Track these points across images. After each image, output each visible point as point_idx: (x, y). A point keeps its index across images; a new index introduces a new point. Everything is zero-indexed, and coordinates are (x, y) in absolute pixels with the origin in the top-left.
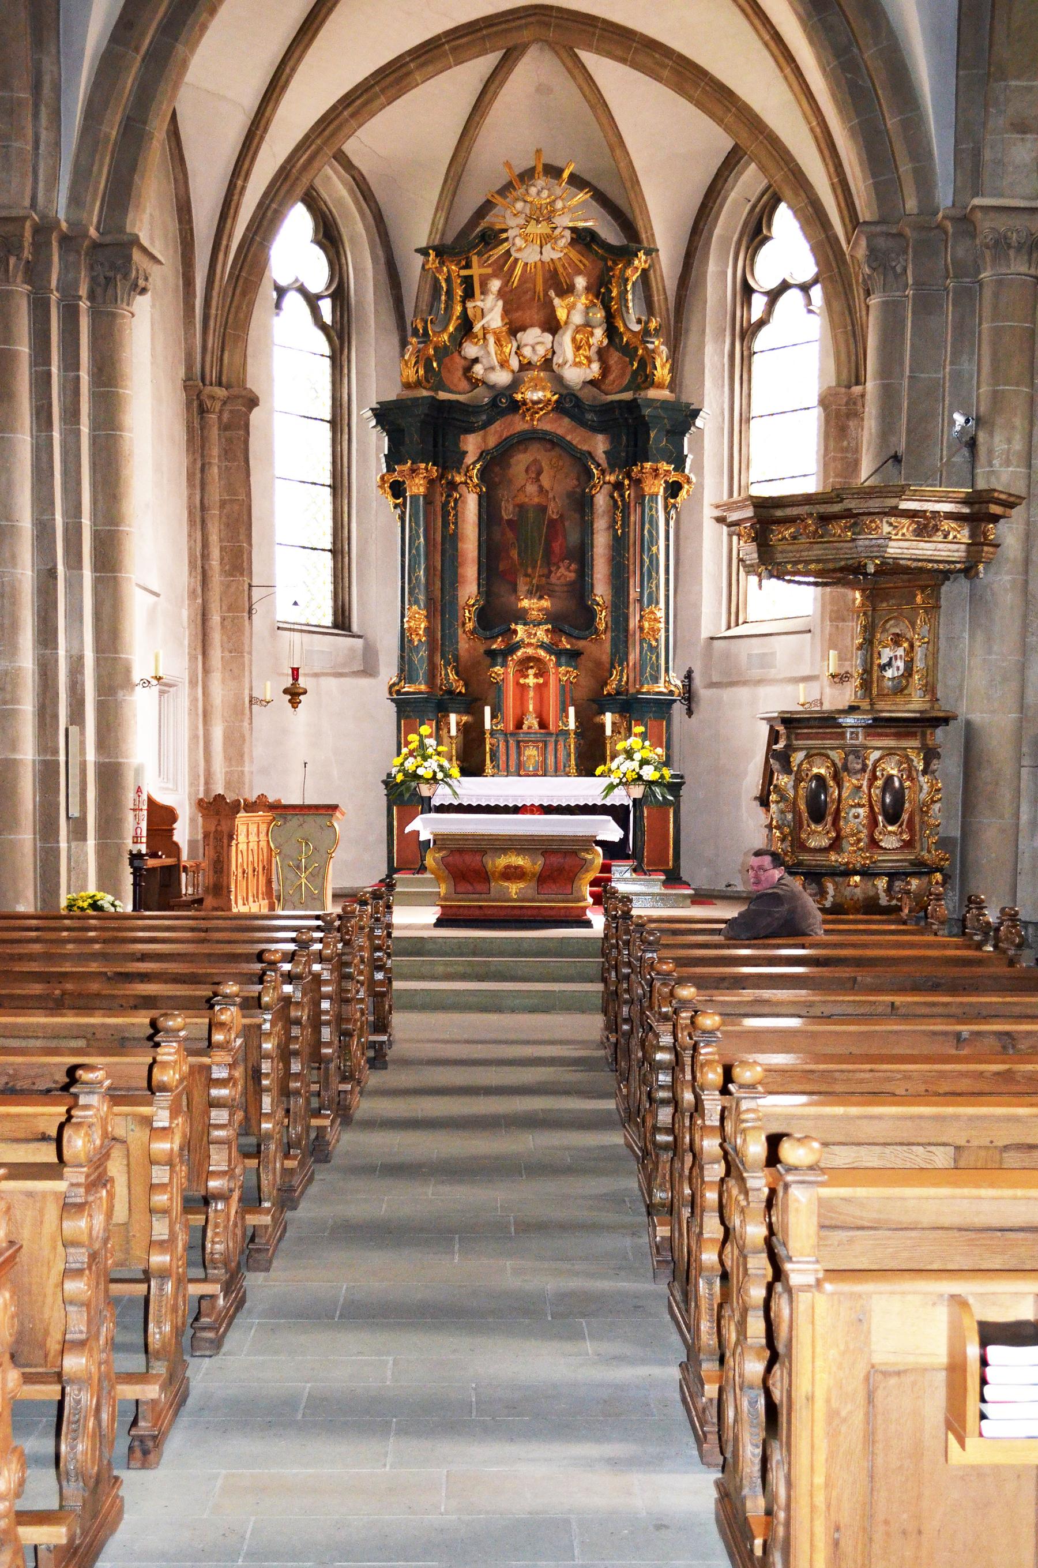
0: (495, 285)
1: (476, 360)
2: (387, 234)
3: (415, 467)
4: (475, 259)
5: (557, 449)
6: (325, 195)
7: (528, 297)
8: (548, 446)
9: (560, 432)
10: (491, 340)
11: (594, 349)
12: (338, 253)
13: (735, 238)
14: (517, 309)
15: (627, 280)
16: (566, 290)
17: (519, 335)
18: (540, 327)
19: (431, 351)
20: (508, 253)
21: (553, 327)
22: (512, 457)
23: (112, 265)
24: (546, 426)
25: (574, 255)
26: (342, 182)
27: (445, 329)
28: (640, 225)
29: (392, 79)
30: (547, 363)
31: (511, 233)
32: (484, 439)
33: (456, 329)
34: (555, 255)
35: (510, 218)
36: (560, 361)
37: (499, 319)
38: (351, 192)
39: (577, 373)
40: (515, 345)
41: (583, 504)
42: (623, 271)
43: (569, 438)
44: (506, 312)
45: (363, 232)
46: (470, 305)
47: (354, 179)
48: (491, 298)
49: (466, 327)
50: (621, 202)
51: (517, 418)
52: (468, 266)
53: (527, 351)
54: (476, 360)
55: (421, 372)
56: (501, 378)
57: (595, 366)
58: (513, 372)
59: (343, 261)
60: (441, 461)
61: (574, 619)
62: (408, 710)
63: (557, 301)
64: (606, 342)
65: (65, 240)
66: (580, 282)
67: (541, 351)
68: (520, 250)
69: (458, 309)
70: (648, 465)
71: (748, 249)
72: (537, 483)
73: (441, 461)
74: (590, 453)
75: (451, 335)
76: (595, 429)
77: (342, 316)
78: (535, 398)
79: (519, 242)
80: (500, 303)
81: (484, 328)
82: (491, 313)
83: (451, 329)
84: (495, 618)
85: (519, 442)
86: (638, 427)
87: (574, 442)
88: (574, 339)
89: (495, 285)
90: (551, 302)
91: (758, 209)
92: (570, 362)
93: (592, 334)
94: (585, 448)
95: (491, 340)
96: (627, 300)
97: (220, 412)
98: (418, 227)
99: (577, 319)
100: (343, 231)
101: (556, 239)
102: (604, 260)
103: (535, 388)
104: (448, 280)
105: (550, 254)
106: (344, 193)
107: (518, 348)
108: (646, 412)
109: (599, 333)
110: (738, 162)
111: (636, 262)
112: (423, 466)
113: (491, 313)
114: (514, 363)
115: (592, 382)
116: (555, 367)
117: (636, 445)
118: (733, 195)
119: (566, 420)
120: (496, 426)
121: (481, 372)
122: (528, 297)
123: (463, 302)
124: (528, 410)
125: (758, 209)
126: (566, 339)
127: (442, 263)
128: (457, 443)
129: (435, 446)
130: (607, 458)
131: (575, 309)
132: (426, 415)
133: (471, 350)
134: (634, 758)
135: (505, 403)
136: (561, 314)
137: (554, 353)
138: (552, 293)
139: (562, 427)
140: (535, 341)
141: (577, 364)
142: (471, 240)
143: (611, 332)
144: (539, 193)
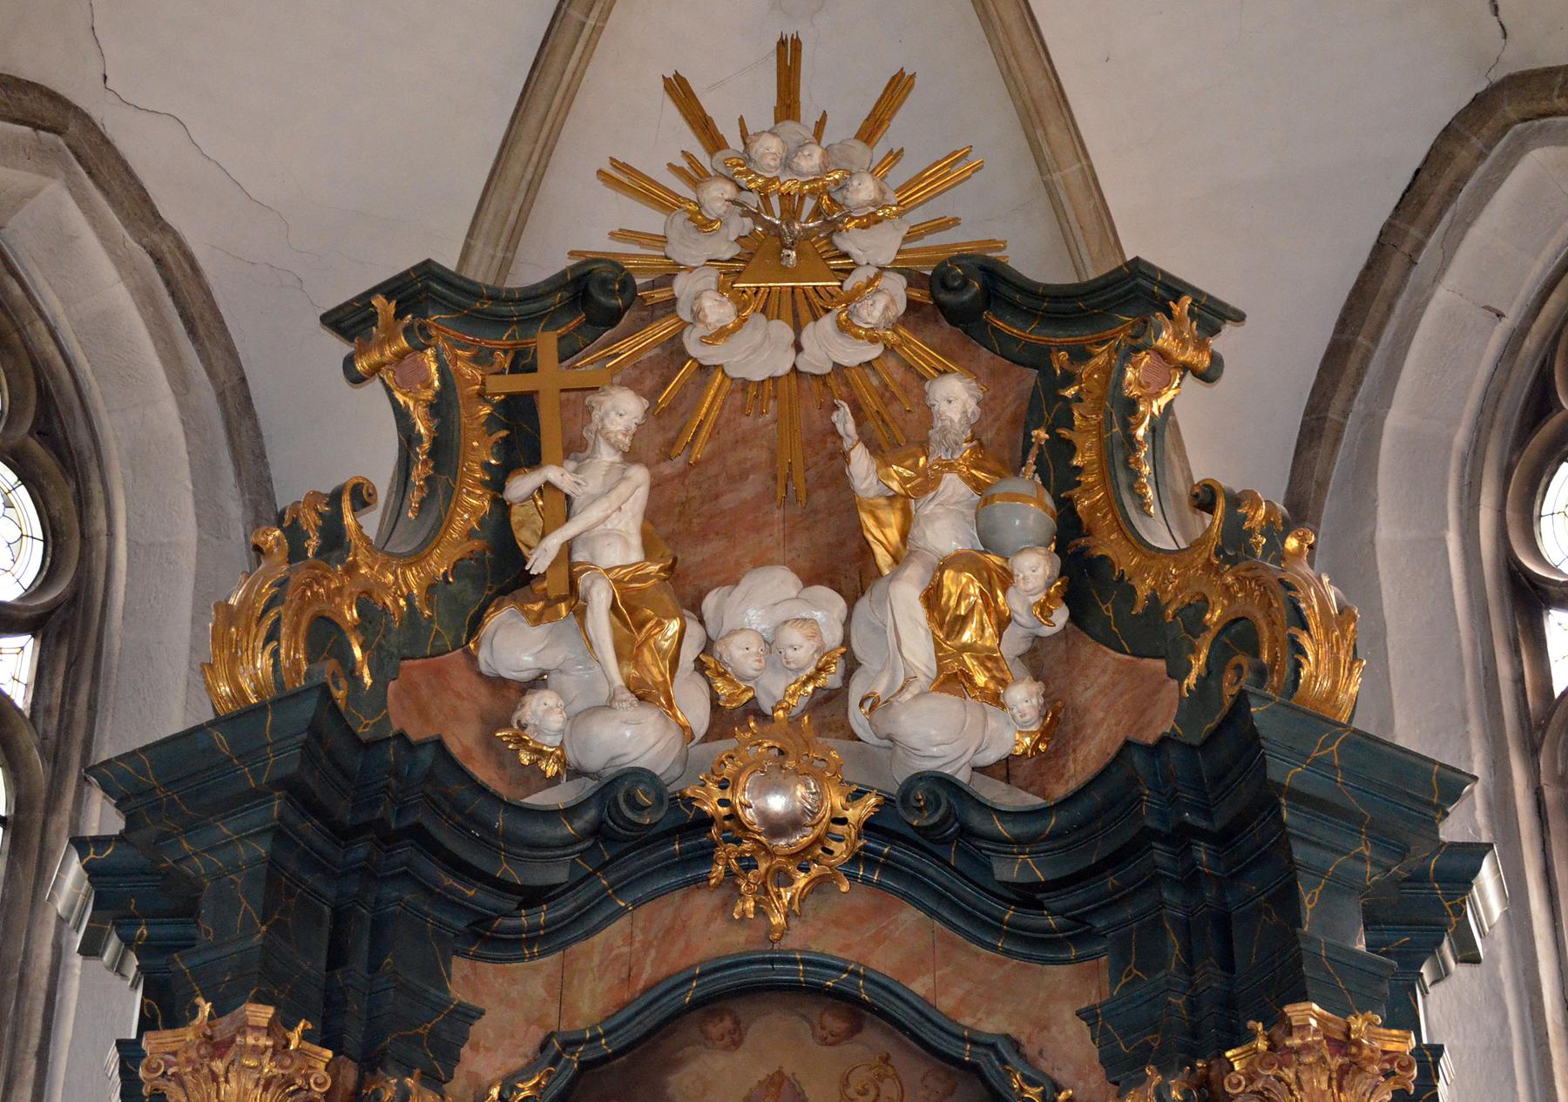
0: (622, 411)
1: (538, 682)
2: (261, 456)
3: (225, 1025)
4: (546, 343)
5: (874, 1039)
6: (51, 302)
7: (750, 489)
8: (837, 1025)
9: (883, 962)
10: (600, 597)
11: (1013, 644)
12: (82, 502)
13: (1461, 437)
14: (703, 536)
15: (1131, 405)
16: (899, 431)
17: (710, 603)
18: (797, 572)
19: (351, 614)
20: (674, 351)
21: (848, 570)
22: (675, 1064)
24: (829, 945)
25: (919, 349)
26: (119, 261)
27: (416, 557)
30: (828, 706)
31: (682, 286)
32: (560, 990)
33: (457, 568)
34: (854, 353)
36: (880, 689)
37: (636, 541)
38: (145, 298)
39: (946, 736)
40: (694, 632)
42: (1113, 378)
43: (919, 986)
44: (663, 524)
45: (178, 430)
46: (521, 486)
47: (159, 261)
48: (607, 456)
49: (501, 571)
51: (703, 902)
52: (523, 363)
53: (741, 654)
54: (538, 682)
55: (293, 652)
56: (635, 739)
57: (1024, 697)
58: (686, 731)
59: (101, 523)
60: (354, 1036)
63: (861, 465)
64: (1061, 616)
66: (955, 399)
67: (801, 650)
68: (723, 333)
69: (474, 503)
70: (1309, 1014)
71: (1506, 475)
73: (354, 1036)
74: (1015, 1045)
75: (431, 588)
76: (1039, 946)
77: (70, 691)
78: (777, 803)
79: (718, 311)
80: (639, 475)
81: (568, 548)
82: (603, 513)
83: (439, 564)
85: (709, 1004)
87: (946, 1003)
88: (932, 597)
89: (622, 411)
90: (846, 457)
91: (1530, 343)
92: (922, 682)
93: (1006, 579)
94: (991, 1025)
95: (600, 597)
96: (1135, 475)
99: (945, 529)
100: (110, 427)
101: (852, 298)
102: (1038, 359)
103: (775, 775)
104: (442, 408)
105: (826, 346)
106: (118, 295)
107: (708, 646)
108: (1285, 772)
109: (1035, 570)
110: (1454, 191)
111: (1165, 339)
112: (262, 1014)
113: (603, 513)
114: (695, 709)
115: (1005, 769)
116: (858, 718)
117: (1228, 965)
118: (1442, 296)
119: (909, 916)
120: (613, 936)
121: (556, 721)
122: (750, 489)
123: (497, 483)
124: (749, 864)
125: (1530, 343)
126: (906, 594)
127: (420, 338)
128: (439, 980)
129: (337, 956)
130: (1101, 1037)
132: (293, 788)
133: (512, 643)
135: (648, 835)
136: (882, 534)
137: (852, 665)
138: (844, 421)
139: (897, 944)
140: (771, 621)
141: (952, 680)
143: (1083, 579)
144: (787, 164)
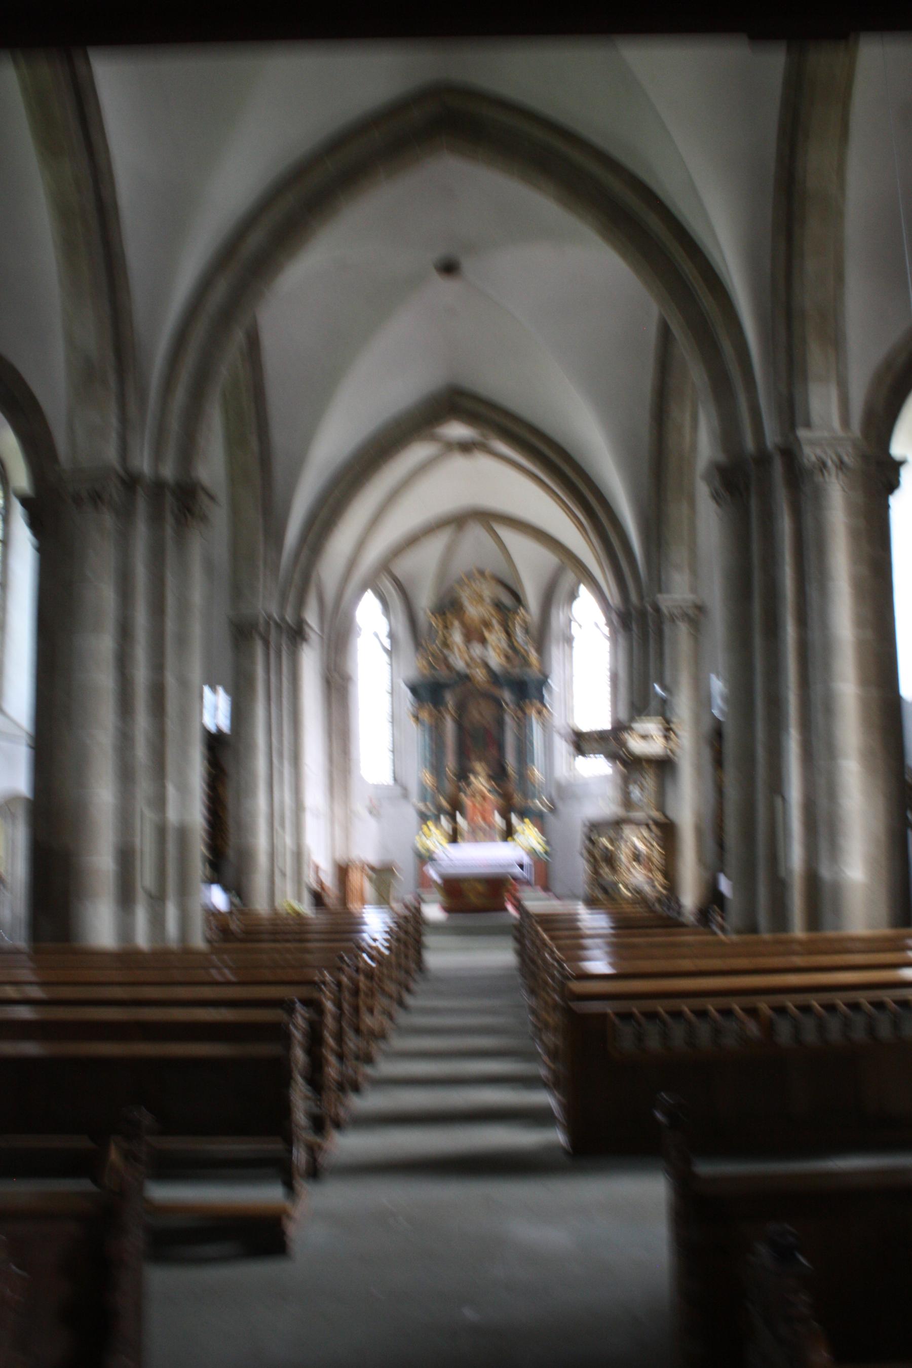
23: (297, 634)
28: (521, 596)
29: (412, 541)
35: (465, 597)
41: (501, 723)
50: (514, 587)
61: (499, 775)
62: (424, 818)
65: (278, 626)
72: (480, 713)
82: (457, 637)
84: (463, 774)
86: (526, 688)
97: (337, 686)
98: (425, 600)
131: (496, 637)
134: (529, 836)
140: (477, 650)
142: (449, 606)
